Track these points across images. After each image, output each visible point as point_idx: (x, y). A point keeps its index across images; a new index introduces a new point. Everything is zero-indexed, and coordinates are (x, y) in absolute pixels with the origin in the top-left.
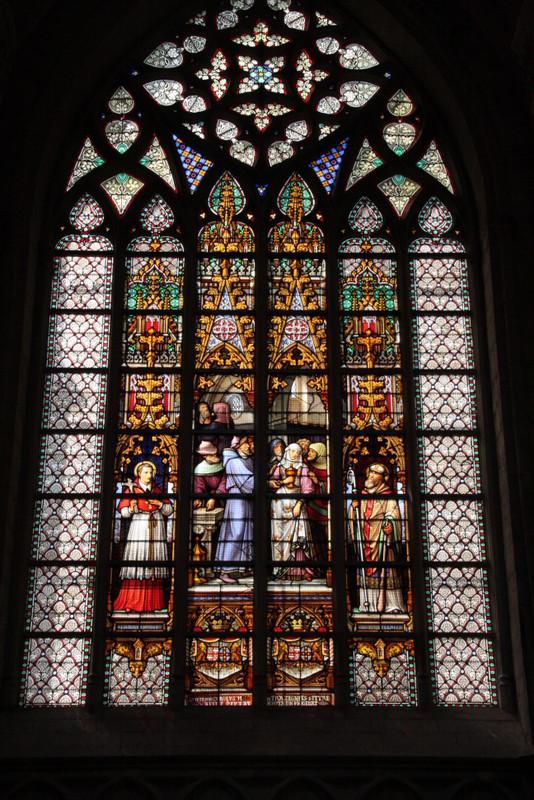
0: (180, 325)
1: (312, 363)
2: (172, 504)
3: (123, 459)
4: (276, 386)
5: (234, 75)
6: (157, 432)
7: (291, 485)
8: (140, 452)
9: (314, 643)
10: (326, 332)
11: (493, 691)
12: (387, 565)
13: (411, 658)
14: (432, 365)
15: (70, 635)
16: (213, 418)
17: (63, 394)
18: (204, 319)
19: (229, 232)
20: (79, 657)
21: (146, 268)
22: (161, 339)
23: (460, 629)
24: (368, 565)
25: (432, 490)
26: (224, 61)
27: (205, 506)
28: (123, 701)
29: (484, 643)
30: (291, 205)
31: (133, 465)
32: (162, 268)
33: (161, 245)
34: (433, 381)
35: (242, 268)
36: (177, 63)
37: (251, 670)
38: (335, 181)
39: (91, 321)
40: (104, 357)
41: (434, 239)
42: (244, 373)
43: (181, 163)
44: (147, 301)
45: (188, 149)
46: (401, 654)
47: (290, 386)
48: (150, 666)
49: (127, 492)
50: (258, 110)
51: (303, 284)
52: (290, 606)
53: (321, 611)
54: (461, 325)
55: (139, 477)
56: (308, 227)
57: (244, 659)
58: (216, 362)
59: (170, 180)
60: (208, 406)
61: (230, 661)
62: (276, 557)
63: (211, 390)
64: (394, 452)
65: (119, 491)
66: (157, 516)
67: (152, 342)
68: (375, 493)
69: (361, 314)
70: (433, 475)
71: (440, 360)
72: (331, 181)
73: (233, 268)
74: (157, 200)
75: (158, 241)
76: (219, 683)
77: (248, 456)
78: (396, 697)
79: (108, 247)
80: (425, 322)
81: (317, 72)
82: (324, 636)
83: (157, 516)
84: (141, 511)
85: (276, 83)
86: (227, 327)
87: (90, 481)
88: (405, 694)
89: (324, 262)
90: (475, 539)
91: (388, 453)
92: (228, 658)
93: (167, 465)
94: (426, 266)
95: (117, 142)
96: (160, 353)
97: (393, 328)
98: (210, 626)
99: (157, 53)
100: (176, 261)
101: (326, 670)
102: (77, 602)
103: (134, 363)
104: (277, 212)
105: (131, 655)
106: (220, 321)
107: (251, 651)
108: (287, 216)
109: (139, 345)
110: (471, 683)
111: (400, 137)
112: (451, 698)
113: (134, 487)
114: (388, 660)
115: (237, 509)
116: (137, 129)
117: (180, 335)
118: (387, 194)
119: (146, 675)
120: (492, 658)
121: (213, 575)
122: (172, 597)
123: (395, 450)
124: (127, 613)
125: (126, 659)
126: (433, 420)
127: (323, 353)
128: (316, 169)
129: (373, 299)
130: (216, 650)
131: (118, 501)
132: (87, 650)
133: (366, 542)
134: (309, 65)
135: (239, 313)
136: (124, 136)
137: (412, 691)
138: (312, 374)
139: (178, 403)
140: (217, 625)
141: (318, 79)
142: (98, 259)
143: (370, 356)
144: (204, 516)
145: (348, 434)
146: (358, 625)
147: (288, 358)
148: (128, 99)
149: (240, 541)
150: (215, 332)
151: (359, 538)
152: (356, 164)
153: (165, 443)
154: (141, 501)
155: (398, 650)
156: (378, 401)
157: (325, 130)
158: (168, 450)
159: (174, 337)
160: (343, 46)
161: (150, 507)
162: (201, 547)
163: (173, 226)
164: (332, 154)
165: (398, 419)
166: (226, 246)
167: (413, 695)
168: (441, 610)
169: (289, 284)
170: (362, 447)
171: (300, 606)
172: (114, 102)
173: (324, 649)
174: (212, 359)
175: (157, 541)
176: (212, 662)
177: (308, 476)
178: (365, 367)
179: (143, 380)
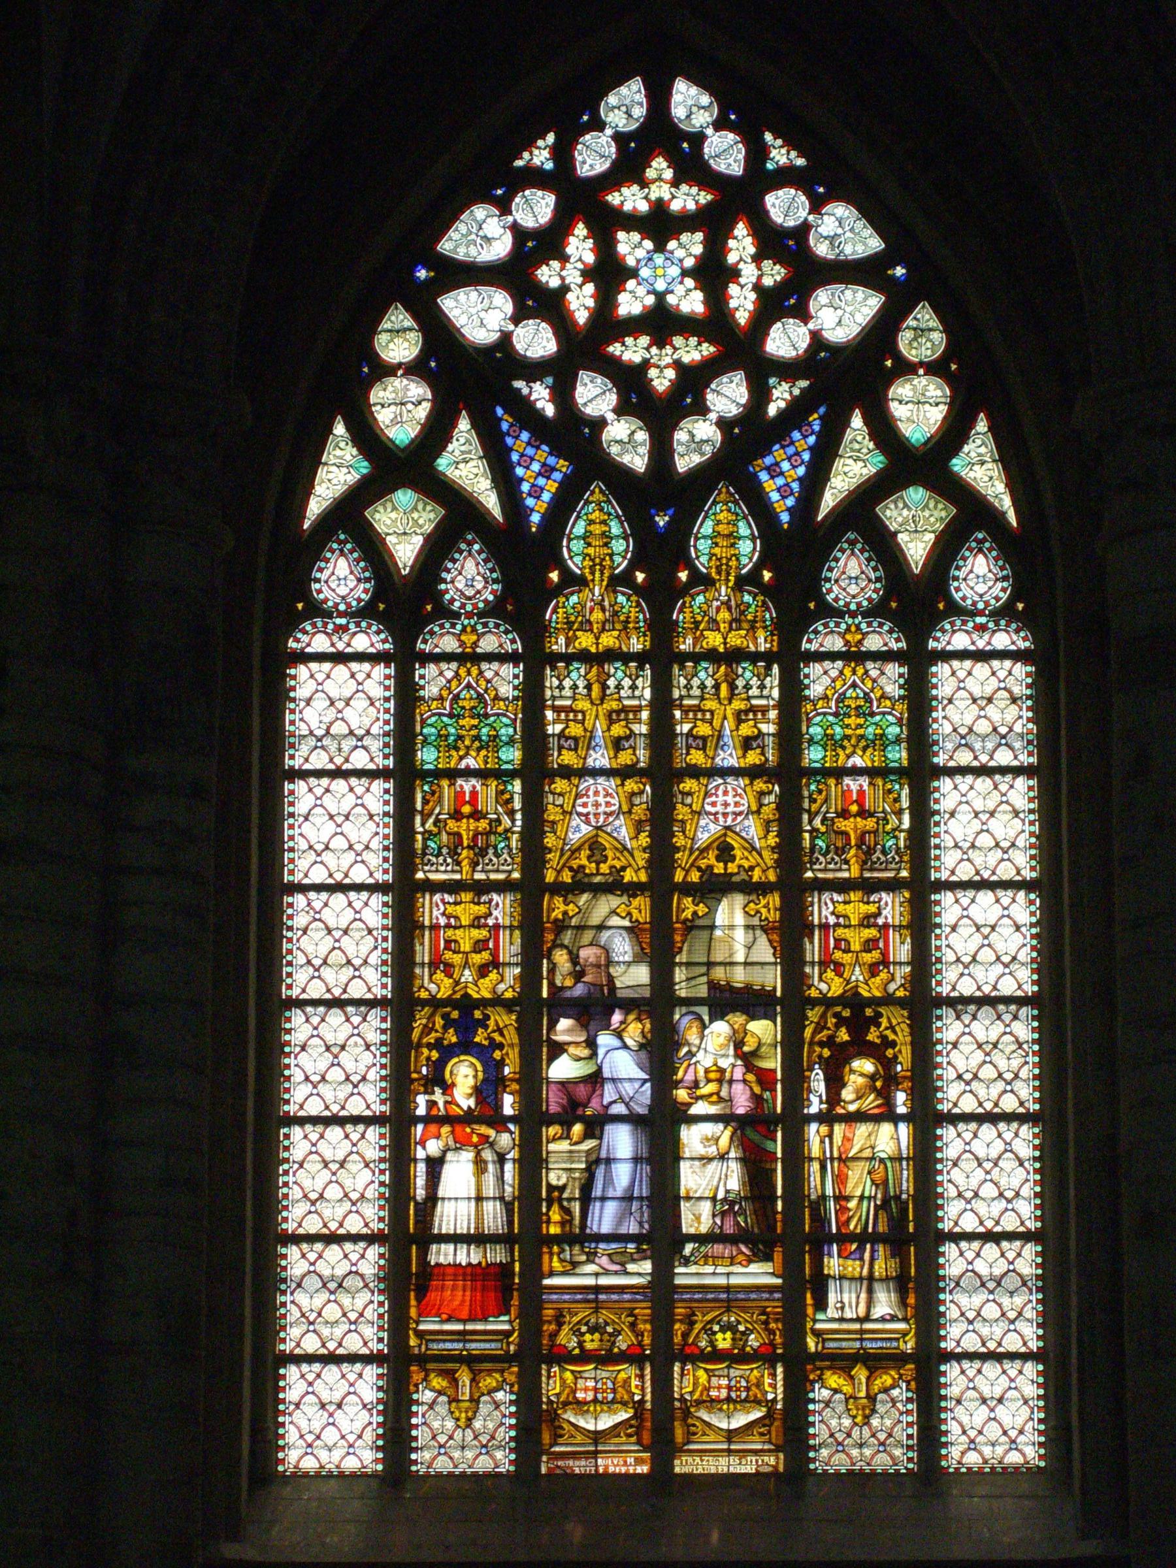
0: (517, 798)
1: (752, 868)
2: (511, 1133)
3: (425, 1051)
6: (483, 1003)
7: (714, 1098)
8: (454, 1039)
10: (777, 809)
11: (1040, 1445)
12: (875, 1238)
13: (910, 1395)
14: (965, 873)
15: (352, 1358)
16: (578, 976)
19: (603, 610)
21: (454, 683)
22: (483, 825)
24: (843, 1238)
27: (568, 1137)
28: (443, 1465)
33: (480, 636)
34: (965, 901)
35: (627, 682)
37: (648, 1415)
38: (798, 500)
40: (386, 860)
42: (632, 890)
43: (511, 467)
45: (525, 436)
46: (893, 1387)
47: (712, 912)
48: (484, 1409)
50: (654, 350)
52: (713, 1309)
54: (1021, 791)
55: (453, 1085)
57: (637, 1398)
59: (491, 502)
60: (570, 953)
61: (613, 1401)
62: (688, 1226)
63: (574, 922)
65: (421, 1111)
66: (488, 1155)
67: (468, 829)
68: (858, 1111)
69: (839, 773)
70: (960, 1077)
73: (611, 683)
76: (597, 1437)
77: (642, 1046)
82: (767, 1357)
83: (488, 1155)
84: (461, 1144)
86: (601, 799)
89: (776, 669)
91: (884, 1038)
92: (610, 1396)
93: (501, 1064)
94: (962, 674)
96: (483, 852)
97: (897, 800)
98: (581, 1344)
99: (463, 228)
100: (508, 670)
101: (770, 1415)
103: (437, 871)
104: (690, 566)
107: (648, 1384)
109: (445, 837)
110: (1005, 1433)
112: (972, 1459)
113: (446, 1102)
114: (872, 1398)
117: (518, 816)
118: (893, 527)
119: (477, 1424)
122: (515, 1293)
123: (895, 1033)
124: (442, 1322)
126: (962, 975)
128: (764, 476)
130: (591, 1384)
132: (380, 1383)
133: (841, 1198)
137: (909, 1448)
139: (516, 948)
140: (592, 1342)
142: (366, 666)
143: (856, 856)
145: (813, 1002)
146: (824, 1340)
147: (711, 858)
148: (410, 329)
149: (628, 1198)
150: (580, 809)
151: (829, 1191)
154: (458, 1128)
155: (889, 1382)
156: (868, 941)
158: (502, 1034)
159: (506, 821)
160: (817, 206)
162: (562, 1207)
164: (792, 443)
167: (910, 1454)
169: (712, 712)
170: (837, 1026)
171: (728, 1310)
175: (488, 1199)
176: (585, 1403)
177: (744, 1081)
178: (846, 875)
179: (456, 903)
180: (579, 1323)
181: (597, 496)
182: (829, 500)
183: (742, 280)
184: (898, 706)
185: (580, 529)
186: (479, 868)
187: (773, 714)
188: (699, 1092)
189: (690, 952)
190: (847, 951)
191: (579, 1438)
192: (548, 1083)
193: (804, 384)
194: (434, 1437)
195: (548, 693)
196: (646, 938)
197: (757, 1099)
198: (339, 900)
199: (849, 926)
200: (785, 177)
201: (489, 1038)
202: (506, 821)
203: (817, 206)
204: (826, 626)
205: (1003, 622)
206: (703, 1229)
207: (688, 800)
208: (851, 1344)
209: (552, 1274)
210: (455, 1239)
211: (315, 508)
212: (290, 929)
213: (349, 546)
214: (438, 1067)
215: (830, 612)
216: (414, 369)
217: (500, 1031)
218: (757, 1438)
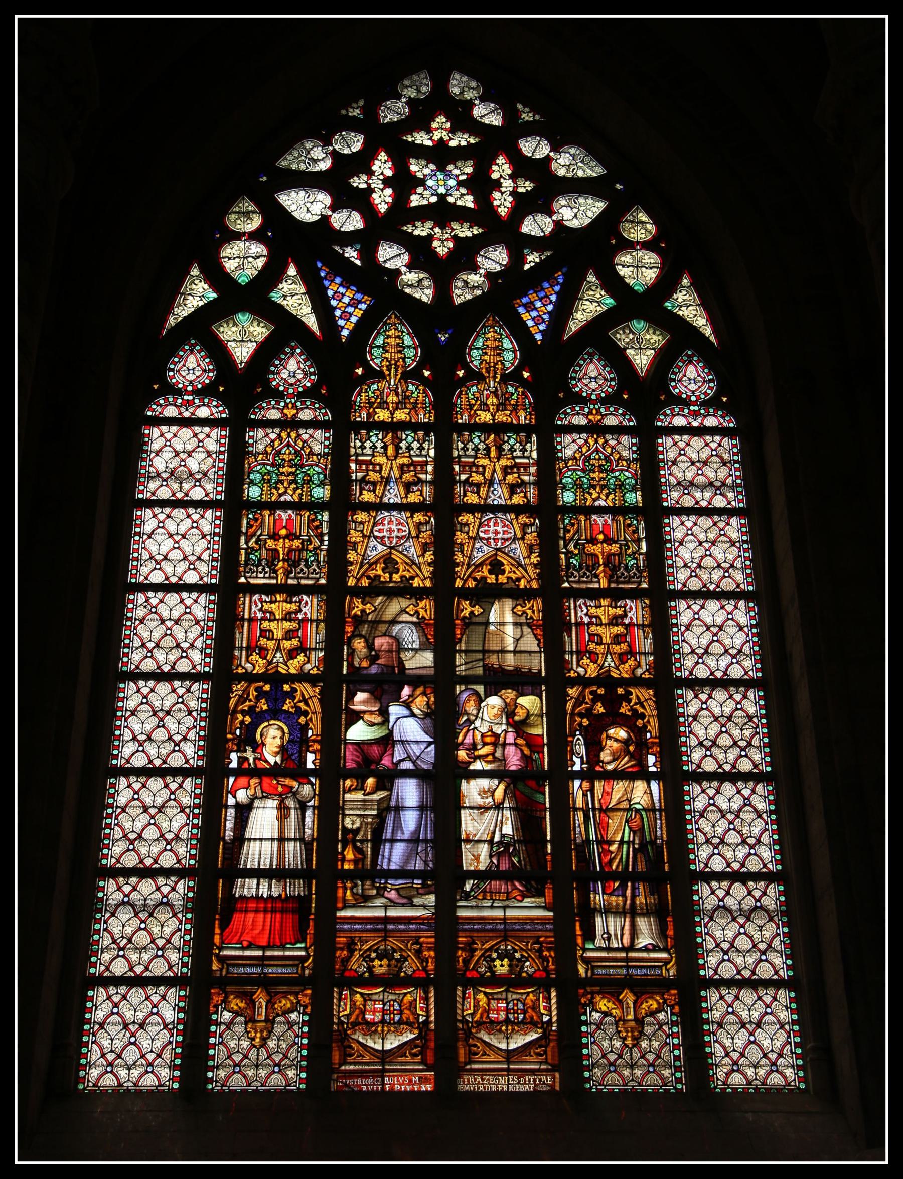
0: (325, 524)
1: (519, 580)
2: (312, 784)
3: (240, 717)
4: (466, 613)
7: (490, 758)
8: (265, 707)
10: (538, 536)
11: (799, 1067)
12: (635, 877)
13: (675, 1019)
15: (157, 981)
16: (373, 659)
18: (361, 516)
19: (397, 395)
20: (169, 1015)
22: (297, 543)
24: (607, 876)
25: (699, 766)
26: (390, 164)
28: (237, 1082)
29: (783, 995)
30: (486, 358)
31: (254, 726)
35: (415, 445)
36: (325, 165)
37: (432, 1036)
38: (548, 326)
39: (195, 517)
40: (214, 568)
41: (692, 408)
42: (419, 594)
43: (327, 299)
44: (277, 489)
46: (659, 1011)
47: (486, 612)
48: (279, 1029)
49: (246, 765)
50: (437, 230)
52: (491, 938)
54: (734, 528)
55: (263, 744)
56: (510, 389)
57: (421, 1019)
59: (311, 321)
60: (366, 641)
61: (400, 1022)
62: (468, 864)
64: (642, 711)
65: (234, 764)
66: (291, 803)
67: (284, 547)
68: (615, 769)
70: (701, 744)
71: (705, 577)
72: (542, 327)
74: (293, 349)
75: (294, 406)
76: (384, 1056)
77: (427, 715)
78: (653, 1078)
80: (682, 524)
81: (520, 182)
82: (541, 984)
83: (291, 803)
85: (462, 195)
86: (394, 527)
87: (189, 749)
88: (666, 1073)
89: (534, 438)
90: (765, 839)
92: (397, 1018)
93: (305, 728)
96: (296, 564)
97: (636, 531)
98: (370, 969)
101: (545, 1036)
102: (168, 931)
103: (257, 577)
104: (466, 367)
106: (384, 518)
109: (264, 552)
110: (765, 1056)
112: (737, 1079)
113: (255, 759)
116: (265, 253)
117: (326, 538)
118: (622, 344)
119: (272, 1044)
120: (795, 1017)
121: (374, 892)
122: (311, 923)
123: (644, 708)
124: (243, 948)
126: (697, 663)
127: (536, 566)
128: (521, 310)
130: (379, 1006)
131: (232, 779)
132: (182, 1004)
133: (604, 842)
134: (509, 172)
135: (412, 508)
137: (677, 1069)
138: (518, 595)
139: (321, 636)
140: (380, 967)
141: (521, 190)
142: (207, 430)
143: (603, 571)
145: (573, 682)
146: (593, 967)
149: (414, 841)
150: (376, 534)
151: (592, 836)
153: (303, 695)
154: (266, 780)
155: (655, 1006)
157: (533, 259)
158: (307, 704)
160: (556, 148)
161: (280, 789)
163: (316, 387)
164: (543, 289)
165: (646, 661)
166: (392, 414)
167: (678, 1075)
168: (718, 945)
170: (594, 701)
171: (505, 939)
172: (233, 217)
173: (542, 1004)
174: (372, 574)
175: (290, 840)
176: (373, 1024)
177: (516, 744)
178: (597, 586)
179: (271, 602)
180: (369, 949)
183: (503, 189)
184: (633, 466)
185: (380, 341)
186: (292, 576)
187: (533, 469)
188: (476, 753)
189: (467, 642)
190: (600, 643)
191: (367, 1058)
192: (346, 743)
194: (229, 1057)
195: (352, 451)
196: (431, 631)
198: (172, 598)
199: (601, 624)
201: (296, 707)
204: (573, 409)
206: (482, 867)
207: (466, 529)
208: (619, 971)
212: (130, 619)
213: (198, 348)
214: (250, 731)
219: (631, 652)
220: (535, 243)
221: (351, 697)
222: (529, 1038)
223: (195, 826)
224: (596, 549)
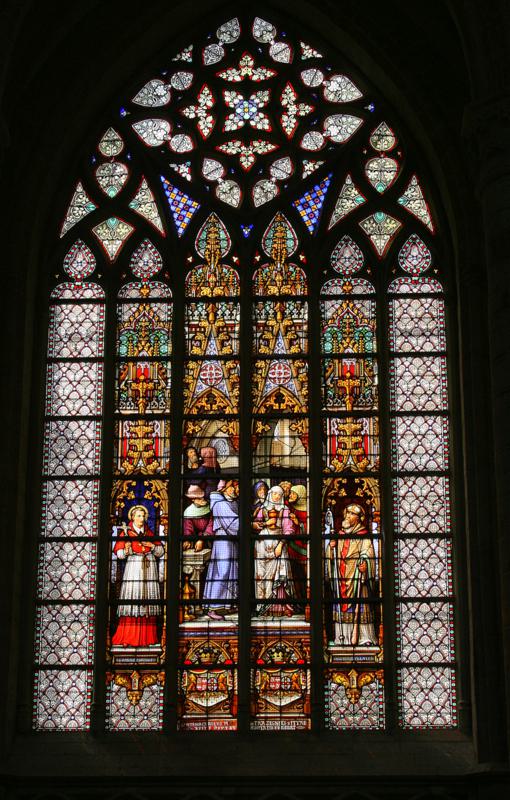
1: (294, 406)
2: (163, 546)
3: (118, 503)
4: (259, 430)
5: (220, 111)
6: (149, 477)
7: (273, 527)
8: (133, 497)
9: (293, 674)
11: (454, 714)
14: (408, 407)
15: (75, 667)
16: (200, 463)
17: (61, 442)
18: (192, 365)
19: (215, 276)
20: (82, 687)
21: (137, 314)
22: (151, 385)
23: (426, 659)
24: (343, 601)
25: (404, 529)
26: (211, 97)
28: (123, 725)
29: (448, 671)
30: (275, 246)
31: (127, 509)
32: (152, 314)
34: (408, 422)
35: (227, 312)
36: (165, 100)
37: (236, 698)
39: (86, 369)
41: (414, 278)
42: (230, 418)
43: (168, 206)
44: (137, 347)
45: (176, 191)
46: (372, 682)
47: (273, 429)
48: (146, 694)
49: (122, 535)
50: (243, 148)
51: (286, 327)
52: (272, 640)
53: (299, 644)
54: (437, 366)
55: (133, 521)
56: (291, 269)
57: (230, 688)
58: (203, 407)
59: (158, 223)
60: (196, 451)
61: (217, 690)
62: (259, 596)
64: (369, 493)
66: (150, 557)
69: (341, 357)
70: (407, 514)
71: (416, 401)
72: (313, 221)
73: (219, 312)
74: (146, 244)
75: (148, 287)
76: (208, 710)
78: (366, 722)
79: (100, 293)
80: (403, 363)
81: (302, 106)
82: (301, 667)
83: (150, 557)
84: (136, 552)
85: (261, 119)
86: (213, 372)
87: (88, 525)
88: (374, 718)
89: (306, 304)
90: (443, 576)
91: (365, 494)
92: (215, 688)
93: (159, 509)
95: (108, 185)
96: (150, 400)
97: (371, 370)
98: (199, 659)
99: (145, 91)
100: (164, 307)
102: (79, 637)
105: (129, 686)
106: (206, 367)
107: (236, 681)
108: (271, 258)
111: (382, 173)
112: (416, 722)
113: (128, 530)
114: (360, 689)
115: (223, 549)
116: (126, 172)
117: (169, 381)
118: (368, 232)
119: (142, 703)
120: (454, 685)
121: (201, 612)
123: (371, 491)
124: (123, 647)
125: (124, 689)
126: (407, 460)
127: (305, 397)
128: (299, 208)
129: (353, 341)
130: (205, 681)
131: (114, 543)
133: (343, 579)
134: (294, 99)
135: (225, 358)
136: (113, 179)
137: (381, 716)
139: (168, 448)
140: (205, 658)
141: (302, 114)
142: (91, 306)
144: (193, 556)
145: (327, 476)
146: (333, 657)
147: (272, 401)
148: (118, 140)
149: (226, 580)
151: (336, 576)
152: (339, 202)
154: (135, 544)
155: (369, 679)
157: (310, 167)
159: (163, 384)
160: (327, 78)
161: (144, 549)
162: (190, 585)
163: (162, 271)
167: (381, 719)
168: (410, 642)
169: (272, 327)
170: (340, 488)
171: (280, 640)
172: (104, 144)
174: (199, 405)
177: (290, 517)
178: (344, 409)
179: (136, 426)
181: (213, 219)
182: (334, 220)
183: (289, 113)
184: (372, 323)
185: (204, 236)
187: (305, 327)
190: (345, 449)
191: (198, 711)
193: (321, 163)
196: (237, 443)
197: (296, 527)
199: (346, 436)
200: (312, 63)
202: (163, 384)
203: (327, 78)
204: (333, 282)
205: (427, 280)
208: (348, 659)
209: (184, 622)
210: (132, 602)
211: (66, 227)
215: (335, 275)
216: (120, 159)
217: (157, 492)
218: (296, 711)
219: (365, 455)
220: (312, 156)
221: (186, 490)
222: (293, 699)
223: (93, 573)
224: (342, 383)
